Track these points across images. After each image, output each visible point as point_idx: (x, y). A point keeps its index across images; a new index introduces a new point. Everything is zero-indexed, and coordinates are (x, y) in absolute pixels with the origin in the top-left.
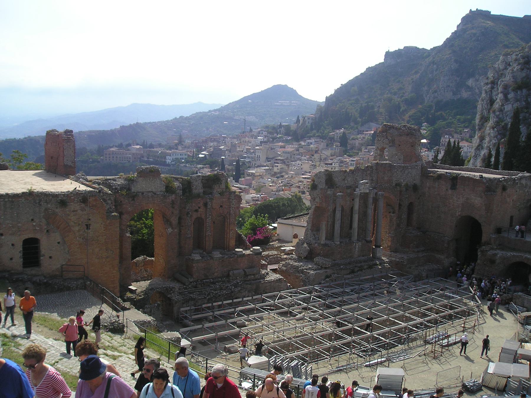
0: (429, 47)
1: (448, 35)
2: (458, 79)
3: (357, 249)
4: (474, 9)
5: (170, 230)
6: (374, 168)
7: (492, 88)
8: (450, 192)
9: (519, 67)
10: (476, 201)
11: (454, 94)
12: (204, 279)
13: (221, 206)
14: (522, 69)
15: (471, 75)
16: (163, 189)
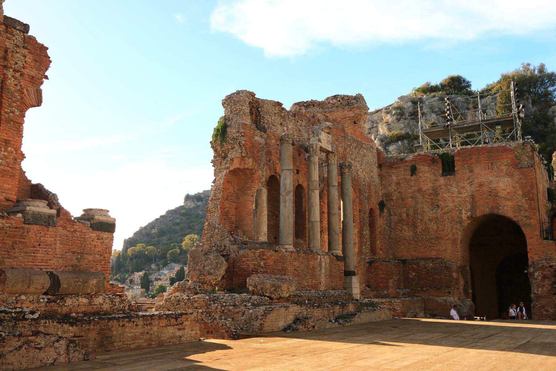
3: (323, 271)
8: (442, 180)
9: (395, 117)
10: (501, 184)
14: (399, 120)
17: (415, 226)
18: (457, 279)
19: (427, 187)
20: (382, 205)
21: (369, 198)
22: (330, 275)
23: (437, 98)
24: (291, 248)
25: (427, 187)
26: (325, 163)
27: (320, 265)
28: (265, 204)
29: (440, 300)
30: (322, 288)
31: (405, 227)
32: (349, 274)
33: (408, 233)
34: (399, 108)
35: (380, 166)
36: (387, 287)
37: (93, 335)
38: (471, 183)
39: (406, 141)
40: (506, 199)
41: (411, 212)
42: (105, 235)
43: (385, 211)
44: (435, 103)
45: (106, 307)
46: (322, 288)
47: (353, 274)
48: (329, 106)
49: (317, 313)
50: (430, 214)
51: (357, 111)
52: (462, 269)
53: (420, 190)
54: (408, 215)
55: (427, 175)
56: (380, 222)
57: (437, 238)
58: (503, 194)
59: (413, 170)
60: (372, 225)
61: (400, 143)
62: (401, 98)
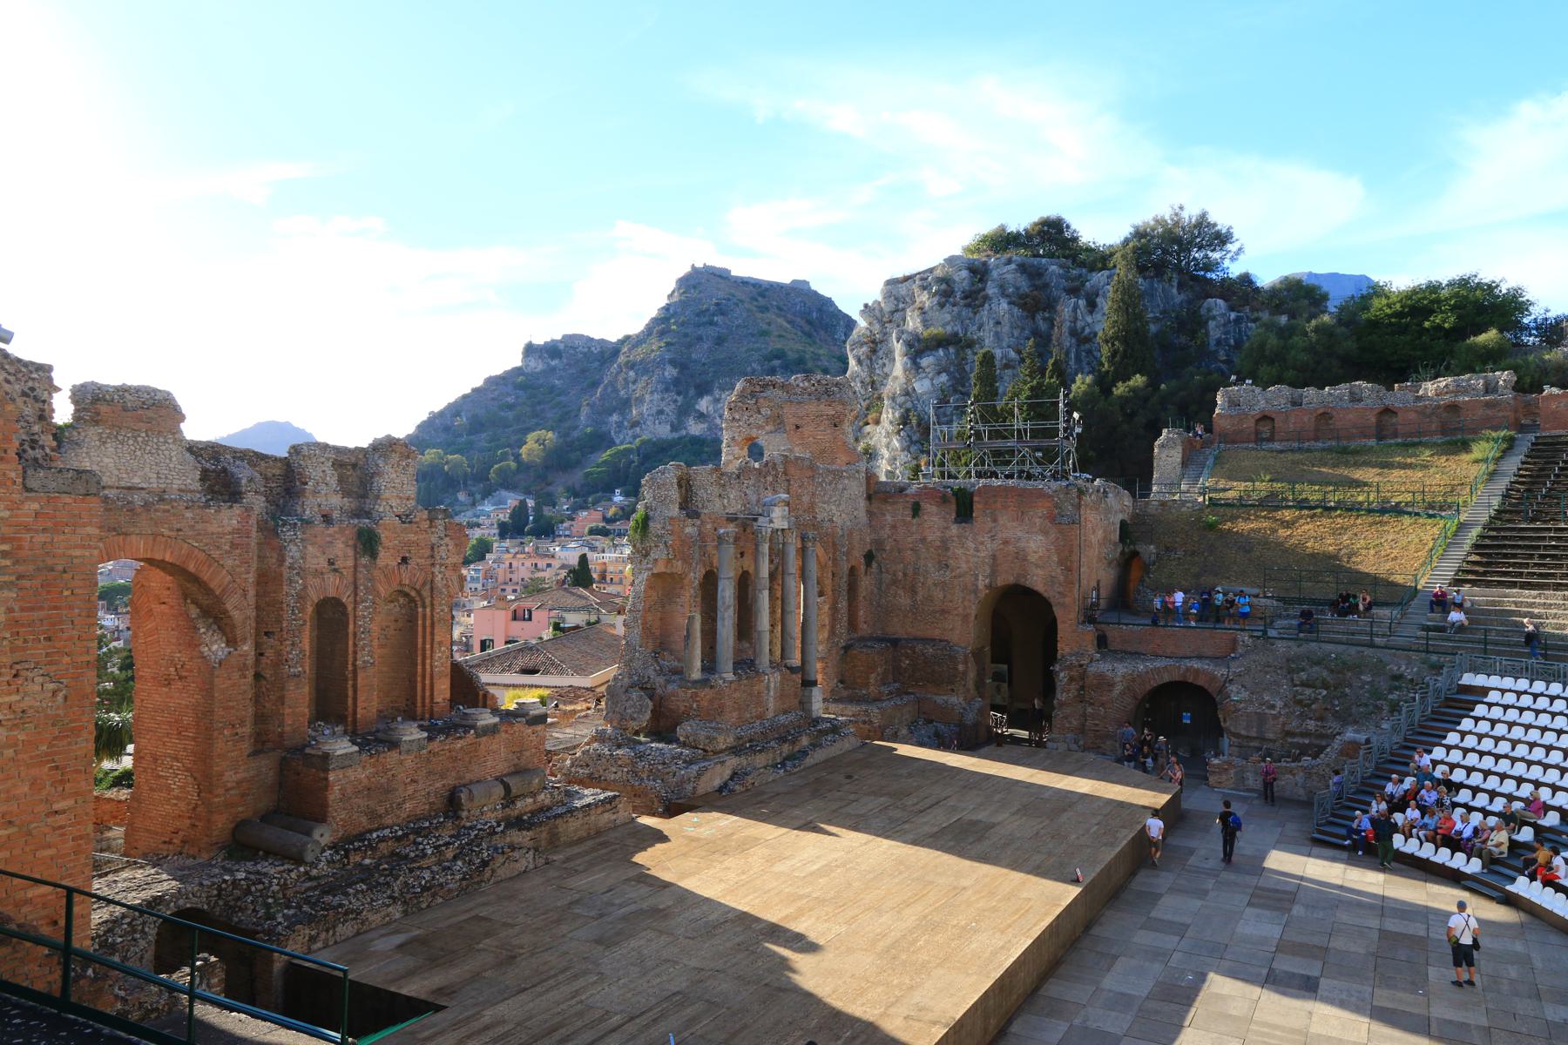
0: (613, 336)
1: (654, 313)
2: (680, 399)
4: (699, 265)
5: (216, 648)
6: (781, 470)
7: (874, 351)
8: (954, 529)
9: (936, 300)
10: (1032, 545)
11: (674, 428)
12: (370, 831)
13: (404, 560)
14: (942, 305)
15: (703, 390)
16: (192, 480)
17: (914, 591)
18: (965, 673)
19: (933, 536)
20: (869, 557)
21: (848, 554)
22: (782, 696)
23: (1013, 266)
24: (730, 676)
25: (933, 536)
26: (778, 555)
27: (768, 688)
28: (698, 634)
29: (939, 699)
30: (770, 714)
31: (901, 592)
32: (809, 683)
33: (904, 600)
34: (945, 280)
35: (869, 498)
36: (867, 685)
37: (544, 835)
38: (993, 538)
39: (952, 350)
40: (1037, 566)
41: (910, 571)
42: (539, 728)
43: (874, 565)
44: (1009, 277)
45: (547, 802)
46: (770, 714)
47: (815, 683)
48: (798, 391)
49: (760, 760)
50: (935, 576)
51: (839, 408)
52: (977, 654)
53: (923, 540)
54: (905, 575)
55: (935, 519)
56: (866, 583)
57: (944, 612)
58: (1033, 558)
59: (916, 510)
60: (852, 588)
61: (941, 352)
62: (951, 261)
